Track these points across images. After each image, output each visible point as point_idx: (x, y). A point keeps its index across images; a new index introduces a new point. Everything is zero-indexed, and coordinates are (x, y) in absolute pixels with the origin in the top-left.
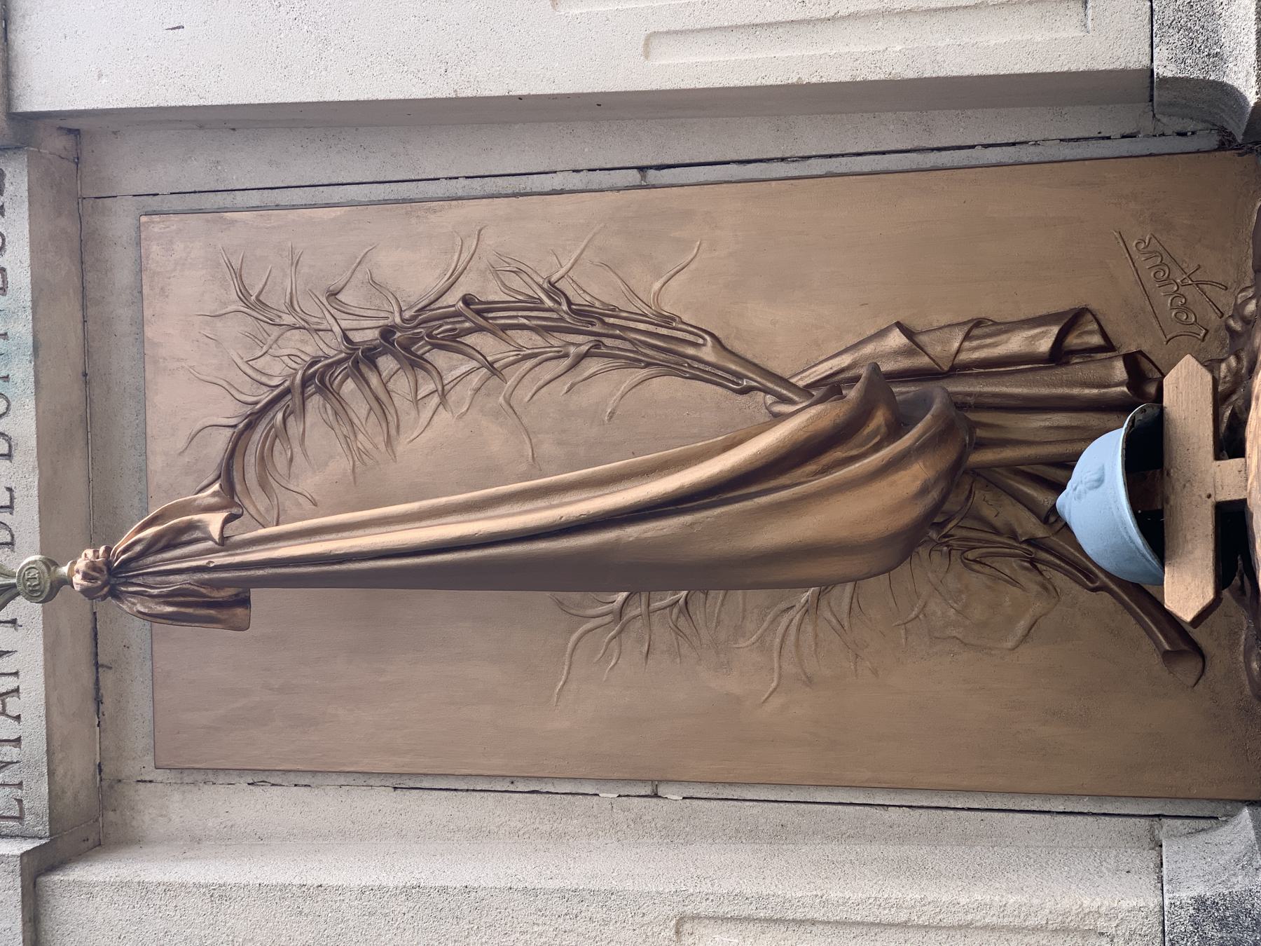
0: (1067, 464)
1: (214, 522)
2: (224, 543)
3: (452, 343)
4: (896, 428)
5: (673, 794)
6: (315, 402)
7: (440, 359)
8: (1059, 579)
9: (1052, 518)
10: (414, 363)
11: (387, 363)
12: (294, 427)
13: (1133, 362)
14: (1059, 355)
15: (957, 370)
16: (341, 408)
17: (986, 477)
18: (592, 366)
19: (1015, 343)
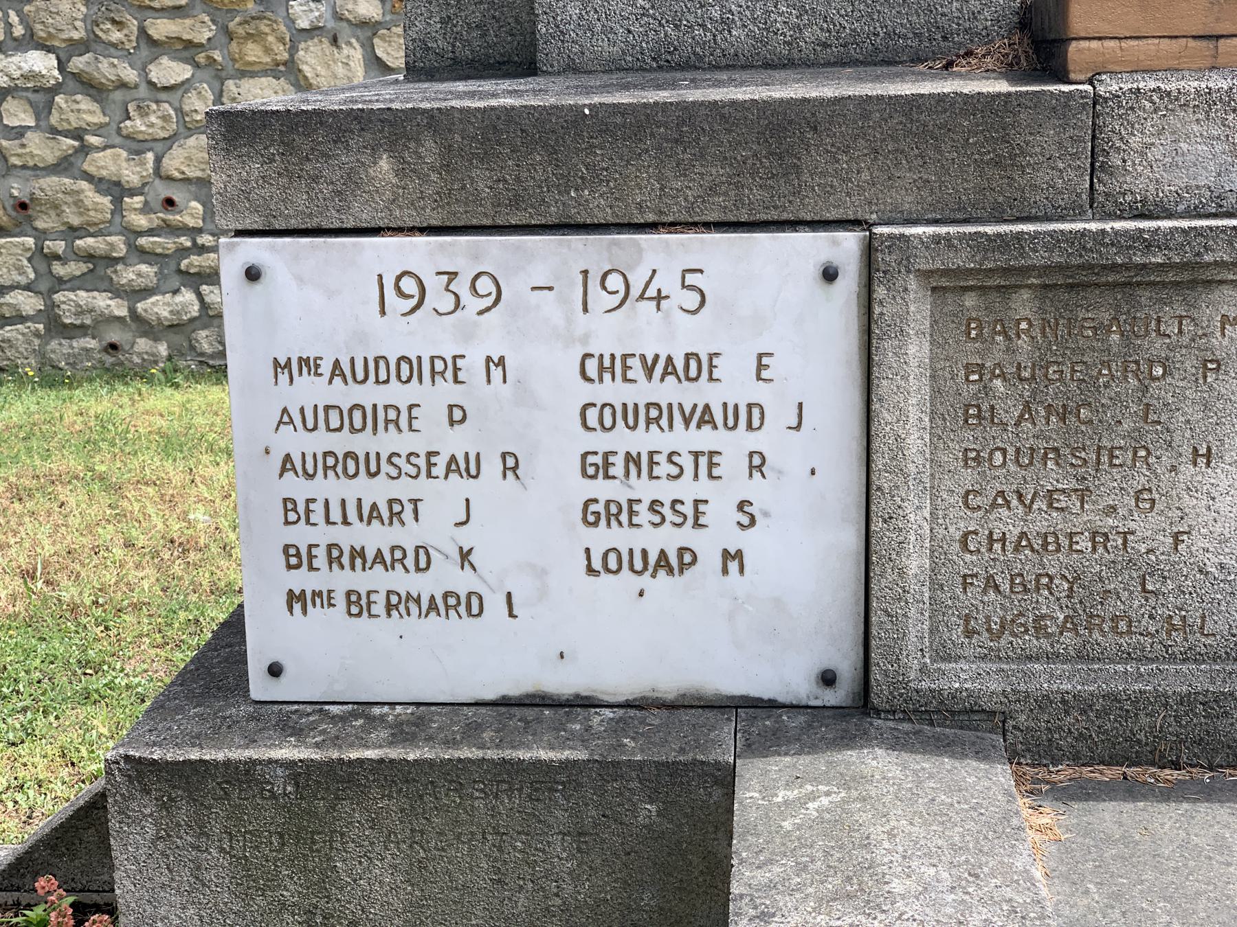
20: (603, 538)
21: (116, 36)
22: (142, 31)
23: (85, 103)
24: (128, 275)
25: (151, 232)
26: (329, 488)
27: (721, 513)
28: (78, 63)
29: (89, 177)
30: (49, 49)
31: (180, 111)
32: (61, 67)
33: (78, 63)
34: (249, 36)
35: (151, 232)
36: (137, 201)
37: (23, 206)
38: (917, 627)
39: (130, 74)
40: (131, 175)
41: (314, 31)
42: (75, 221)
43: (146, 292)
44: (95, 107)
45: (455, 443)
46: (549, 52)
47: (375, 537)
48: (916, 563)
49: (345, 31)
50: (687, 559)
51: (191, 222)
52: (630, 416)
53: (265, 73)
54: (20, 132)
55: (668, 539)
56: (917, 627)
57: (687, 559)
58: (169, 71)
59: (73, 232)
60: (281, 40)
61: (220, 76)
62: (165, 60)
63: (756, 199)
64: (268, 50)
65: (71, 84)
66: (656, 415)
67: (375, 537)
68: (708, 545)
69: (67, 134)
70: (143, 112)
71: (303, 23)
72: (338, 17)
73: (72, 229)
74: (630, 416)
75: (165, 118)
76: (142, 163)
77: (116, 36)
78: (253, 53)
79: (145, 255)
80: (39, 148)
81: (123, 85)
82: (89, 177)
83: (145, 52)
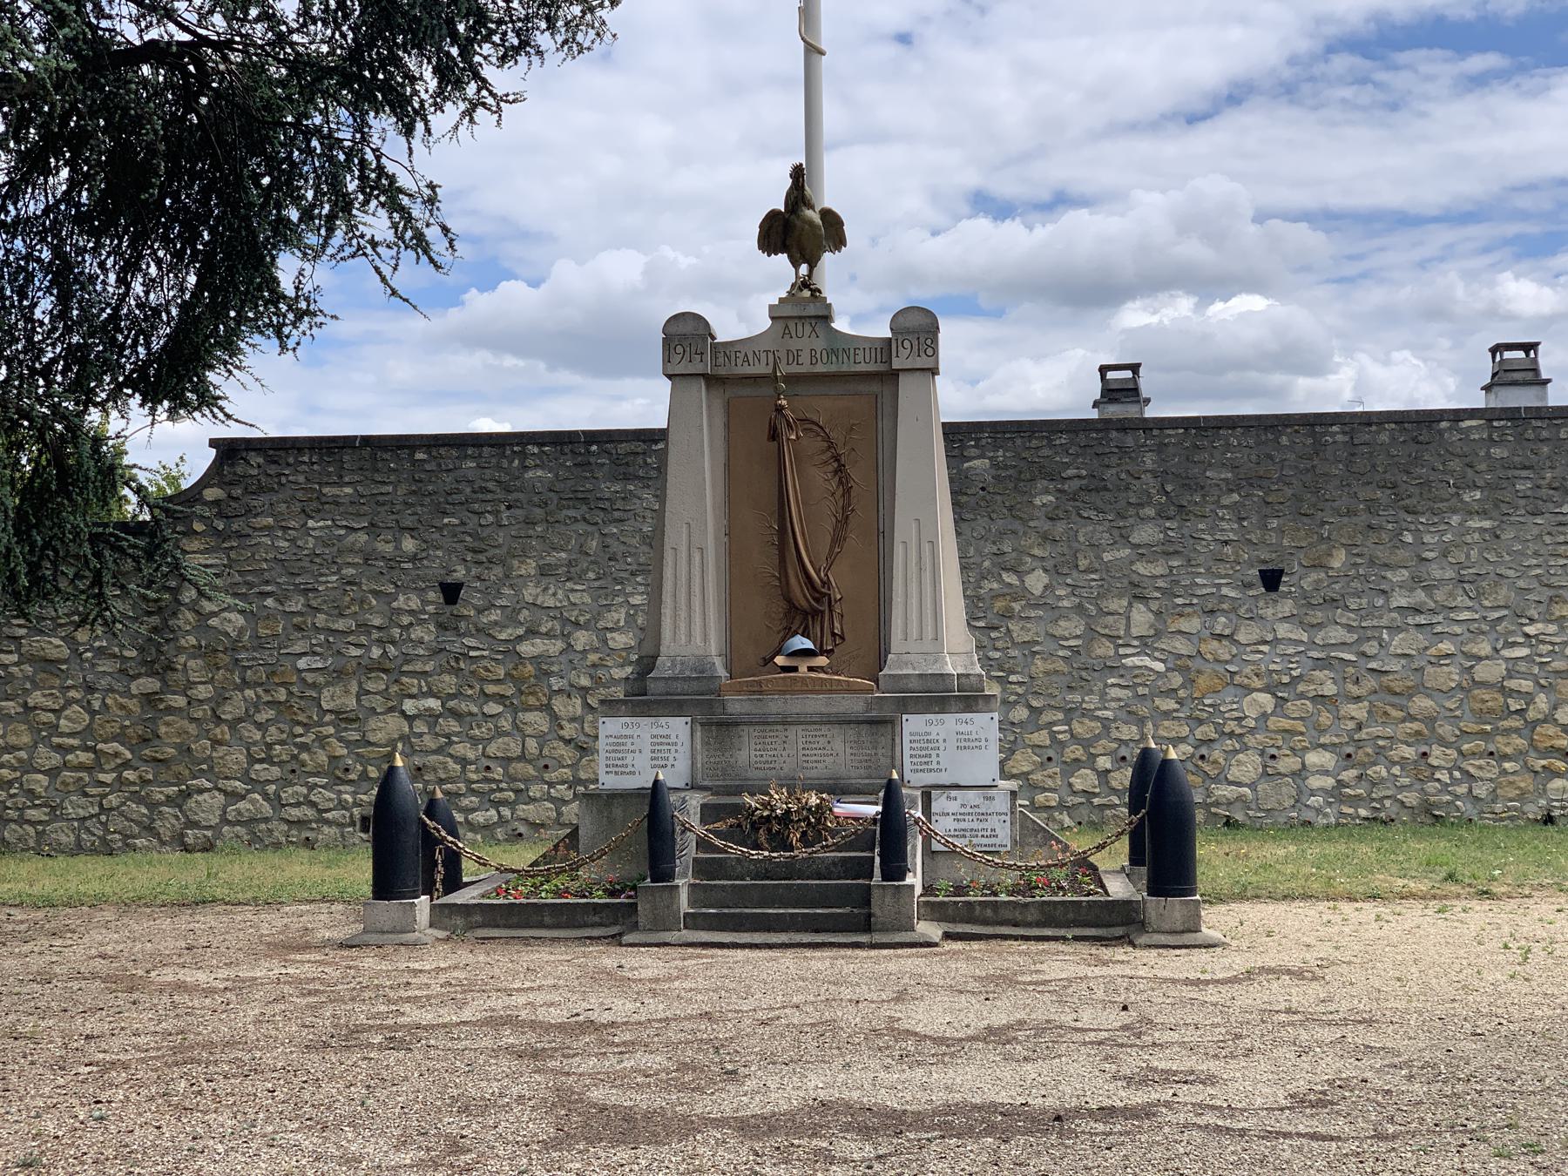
0: (808, 637)
1: (793, 437)
2: (788, 439)
3: (840, 482)
4: (814, 599)
5: (726, 539)
6: (826, 444)
7: (837, 478)
8: (781, 634)
9: (795, 633)
10: (836, 472)
11: (836, 465)
12: (819, 438)
13: (832, 650)
14: (834, 635)
15: (831, 611)
16: (823, 452)
17: (805, 619)
18: (834, 520)
19: (837, 624)
20: (654, 762)
21: (470, 692)
22: (482, 690)
23: (453, 722)
24: (465, 802)
25: (477, 782)
26: (613, 755)
27: (671, 759)
28: (451, 704)
29: (451, 756)
30: (438, 698)
31: (496, 726)
32: (443, 705)
33: (451, 704)
34: (531, 693)
35: (477, 782)
36: (473, 767)
37: (419, 769)
38: (700, 776)
39: (475, 710)
40: (471, 755)
41: (560, 691)
42: (443, 776)
43: (474, 810)
44: (456, 724)
45: (632, 748)
46: (649, 692)
47: (620, 763)
48: (699, 765)
49: (574, 692)
50: (666, 766)
51: (497, 777)
52: (658, 744)
53: (536, 709)
54: (421, 735)
55: (663, 763)
56: (700, 776)
57: (666, 766)
58: (493, 708)
59: (441, 781)
60: (545, 695)
61: (515, 710)
62: (491, 704)
63: (676, 713)
64: (538, 700)
65: (447, 713)
66: (662, 744)
67: (620, 763)
68: (669, 764)
69: (443, 736)
70: (479, 727)
71: (556, 688)
72: (572, 686)
73: (441, 780)
74: (658, 744)
75: (489, 729)
76: (477, 750)
77: (470, 692)
78: (532, 700)
79: (473, 792)
80: (429, 742)
81: (471, 714)
82: (451, 756)
83: (482, 700)
